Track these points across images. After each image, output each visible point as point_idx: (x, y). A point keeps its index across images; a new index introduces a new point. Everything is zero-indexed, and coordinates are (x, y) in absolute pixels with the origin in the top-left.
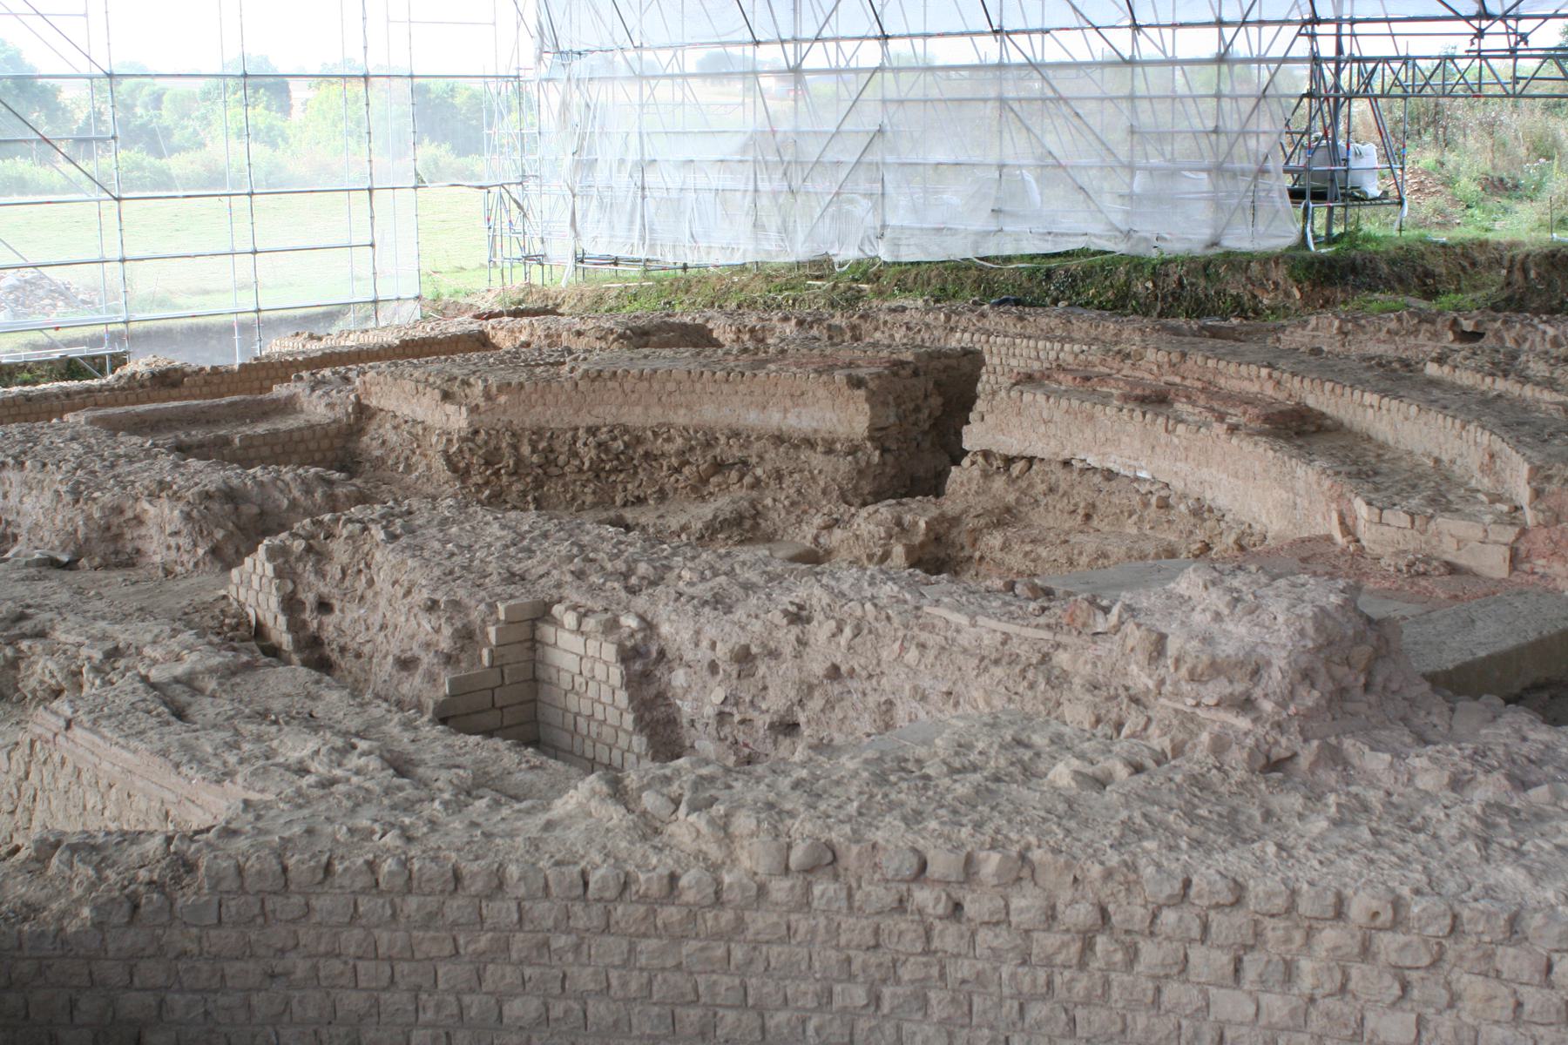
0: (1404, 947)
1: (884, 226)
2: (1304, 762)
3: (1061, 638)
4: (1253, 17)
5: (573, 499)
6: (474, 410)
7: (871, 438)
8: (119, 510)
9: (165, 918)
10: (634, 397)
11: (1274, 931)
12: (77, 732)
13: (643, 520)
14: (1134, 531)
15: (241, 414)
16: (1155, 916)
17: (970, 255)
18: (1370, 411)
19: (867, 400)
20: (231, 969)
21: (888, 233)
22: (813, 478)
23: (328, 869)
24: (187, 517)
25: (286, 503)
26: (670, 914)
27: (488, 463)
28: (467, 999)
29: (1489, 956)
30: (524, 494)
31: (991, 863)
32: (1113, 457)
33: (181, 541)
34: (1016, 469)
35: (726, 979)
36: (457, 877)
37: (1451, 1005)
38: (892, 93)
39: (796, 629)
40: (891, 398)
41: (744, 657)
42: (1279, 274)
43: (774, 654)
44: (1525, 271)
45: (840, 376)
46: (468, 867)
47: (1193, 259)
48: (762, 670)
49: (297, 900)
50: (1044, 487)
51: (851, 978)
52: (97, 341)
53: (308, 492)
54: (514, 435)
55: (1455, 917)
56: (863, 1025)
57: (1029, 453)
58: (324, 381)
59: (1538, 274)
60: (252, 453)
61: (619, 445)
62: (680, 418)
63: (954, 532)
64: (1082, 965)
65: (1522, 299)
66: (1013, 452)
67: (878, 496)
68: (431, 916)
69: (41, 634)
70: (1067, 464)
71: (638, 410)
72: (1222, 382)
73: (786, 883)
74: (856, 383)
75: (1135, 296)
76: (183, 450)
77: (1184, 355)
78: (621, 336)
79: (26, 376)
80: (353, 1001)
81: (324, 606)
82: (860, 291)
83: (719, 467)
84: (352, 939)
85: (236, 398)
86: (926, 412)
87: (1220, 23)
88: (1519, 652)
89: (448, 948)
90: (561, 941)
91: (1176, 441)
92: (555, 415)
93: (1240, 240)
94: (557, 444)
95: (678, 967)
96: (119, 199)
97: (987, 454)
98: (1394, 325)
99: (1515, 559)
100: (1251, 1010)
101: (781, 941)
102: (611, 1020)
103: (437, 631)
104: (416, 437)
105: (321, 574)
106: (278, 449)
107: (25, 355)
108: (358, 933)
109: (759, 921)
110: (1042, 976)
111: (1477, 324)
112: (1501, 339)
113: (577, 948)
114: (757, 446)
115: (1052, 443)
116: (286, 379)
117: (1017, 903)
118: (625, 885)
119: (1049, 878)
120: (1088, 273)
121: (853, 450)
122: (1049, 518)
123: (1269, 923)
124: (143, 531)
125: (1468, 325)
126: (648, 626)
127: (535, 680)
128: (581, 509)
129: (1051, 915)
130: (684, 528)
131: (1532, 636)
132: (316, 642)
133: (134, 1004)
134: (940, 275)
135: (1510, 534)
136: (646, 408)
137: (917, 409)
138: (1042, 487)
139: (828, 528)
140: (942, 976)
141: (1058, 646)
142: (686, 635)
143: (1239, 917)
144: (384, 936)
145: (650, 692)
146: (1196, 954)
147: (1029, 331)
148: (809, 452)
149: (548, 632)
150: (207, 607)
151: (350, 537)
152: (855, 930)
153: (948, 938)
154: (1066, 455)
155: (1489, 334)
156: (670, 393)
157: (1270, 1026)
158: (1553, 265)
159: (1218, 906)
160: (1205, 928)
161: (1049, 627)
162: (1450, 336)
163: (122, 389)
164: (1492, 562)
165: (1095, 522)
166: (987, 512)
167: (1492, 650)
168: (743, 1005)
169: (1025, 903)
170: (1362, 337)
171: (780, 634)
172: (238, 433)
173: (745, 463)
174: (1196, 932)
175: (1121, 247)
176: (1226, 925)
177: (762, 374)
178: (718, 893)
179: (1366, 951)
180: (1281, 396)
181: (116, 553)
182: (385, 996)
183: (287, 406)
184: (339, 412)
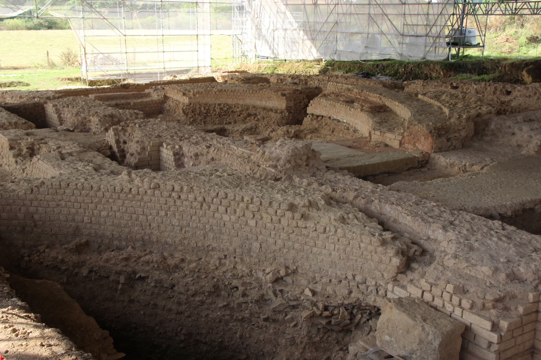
0: (253, 207)
1: (336, 50)
2: (283, 179)
3: (252, 153)
5: (213, 122)
6: (190, 98)
7: (286, 109)
8: (85, 118)
9: (38, 193)
10: (230, 96)
11: (233, 203)
12: (40, 161)
13: (229, 128)
14: (341, 135)
15: (135, 97)
16: (213, 200)
17: (359, 59)
19: (286, 99)
20: (50, 203)
22: (271, 119)
23: (68, 185)
24: (100, 121)
25: (125, 119)
26: (130, 196)
27: (193, 112)
28: (94, 211)
29: (267, 209)
30: (201, 120)
31: (185, 188)
33: (98, 126)
34: (320, 118)
35: (140, 209)
36: (92, 187)
37: (261, 219)
38: (340, 11)
39: (207, 150)
40: (292, 99)
41: (196, 155)
42: (438, 67)
43: (202, 155)
44: (505, 68)
45: (279, 93)
46: (94, 185)
47: (416, 63)
48: (200, 158)
49: (62, 190)
51: (162, 210)
52: (120, 75)
53: (131, 116)
55: (261, 202)
56: (164, 219)
57: (322, 114)
58: (158, 89)
60: (136, 107)
61: (225, 109)
62: (241, 102)
63: (301, 134)
64: (201, 209)
65: (503, 76)
66: (318, 114)
67: (287, 124)
68: (87, 195)
69: (46, 143)
70: (330, 118)
71: (231, 100)
72: (369, 98)
73: (150, 191)
74: (283, 95)
75: (399, 73)
76: (117, 106)
77: (362, 90)
78: (242, 80)
79: (99, 83)
80: (73, 211)
81: (125, 142)
82: (328, 69)
83: (249, 115)
84: (73, 199)
85: (135, 92)
86: (303, 103)
88: (379, 164)
89: (90, 201)
90: (111, 200)
92: (210, 100)
93: (431, 57)
94: (210, 108)
95: (132, 206)
96: (125, 36)
97: (312, 115)
98: (436, 84)
99: (401, 144)
100: (229, 219)
101: (149, 202)
102: (120, 216)
103: (138, 147)
104: (177, 104)
105: (124, 135)
106: (143, 106)
107: (101, 78)
108: (74, 197)
109: (146, 198)
110: (194, 211)
112: (463, 89)
113: (114, 202)
114: (259, 110)
116: (148, 88)
117: (190, 196)
118: (122, 190)
119: (196, 192)
120: (388, 66)
121: (282, 112)
122: (325, 131)
123: (231, 202)
124: (91, 124)
125: (455, 85)
126: (181, 147)
127: (159, 159)
128: (215, 124)
129: (196, 199)
130: (237, 130)
131: (385, 160)
132: (123, 151)
133: (32, 209)
134: (349, 65)
135: (400, 138)
137: (300, 102)
138: (324, 124)
139: (272, 132)
140: (178, 210)
141: (251, 154)
142: (187, 150)
143: (227, 201)
144: (79, 198)
145: (180, 163)
146: (220, 207)
147: (348, 82)
149: (161, 148)
150: (100, 142)
151: (131, 126)
152: (162, 200)
153: (178, 203)
154: (329, 115)
155: (460, 87)
157: (232, 222)
158: (512, 67)
159: (223, 198)
160: (221, 202)
161: (250, 150)
162: (450, 87)
163: (113, 89)
164: (395, 144)
165: (334, 133)
166: (310, 129)
167: (371, 163)
168: (143, 214)
169: (191, 196)
170: (428, 87)
171: (204, 150)
172: (132, 102)
173: (256, 114)
174: (219, 203)
176: (225, 202)
177: (261, 92)
178: (138, 192)
179: (247, 208)
180: (380, 102)
181: (85, 129)
182: (79, 210)
183: (148, 95)
184: (160, 97)
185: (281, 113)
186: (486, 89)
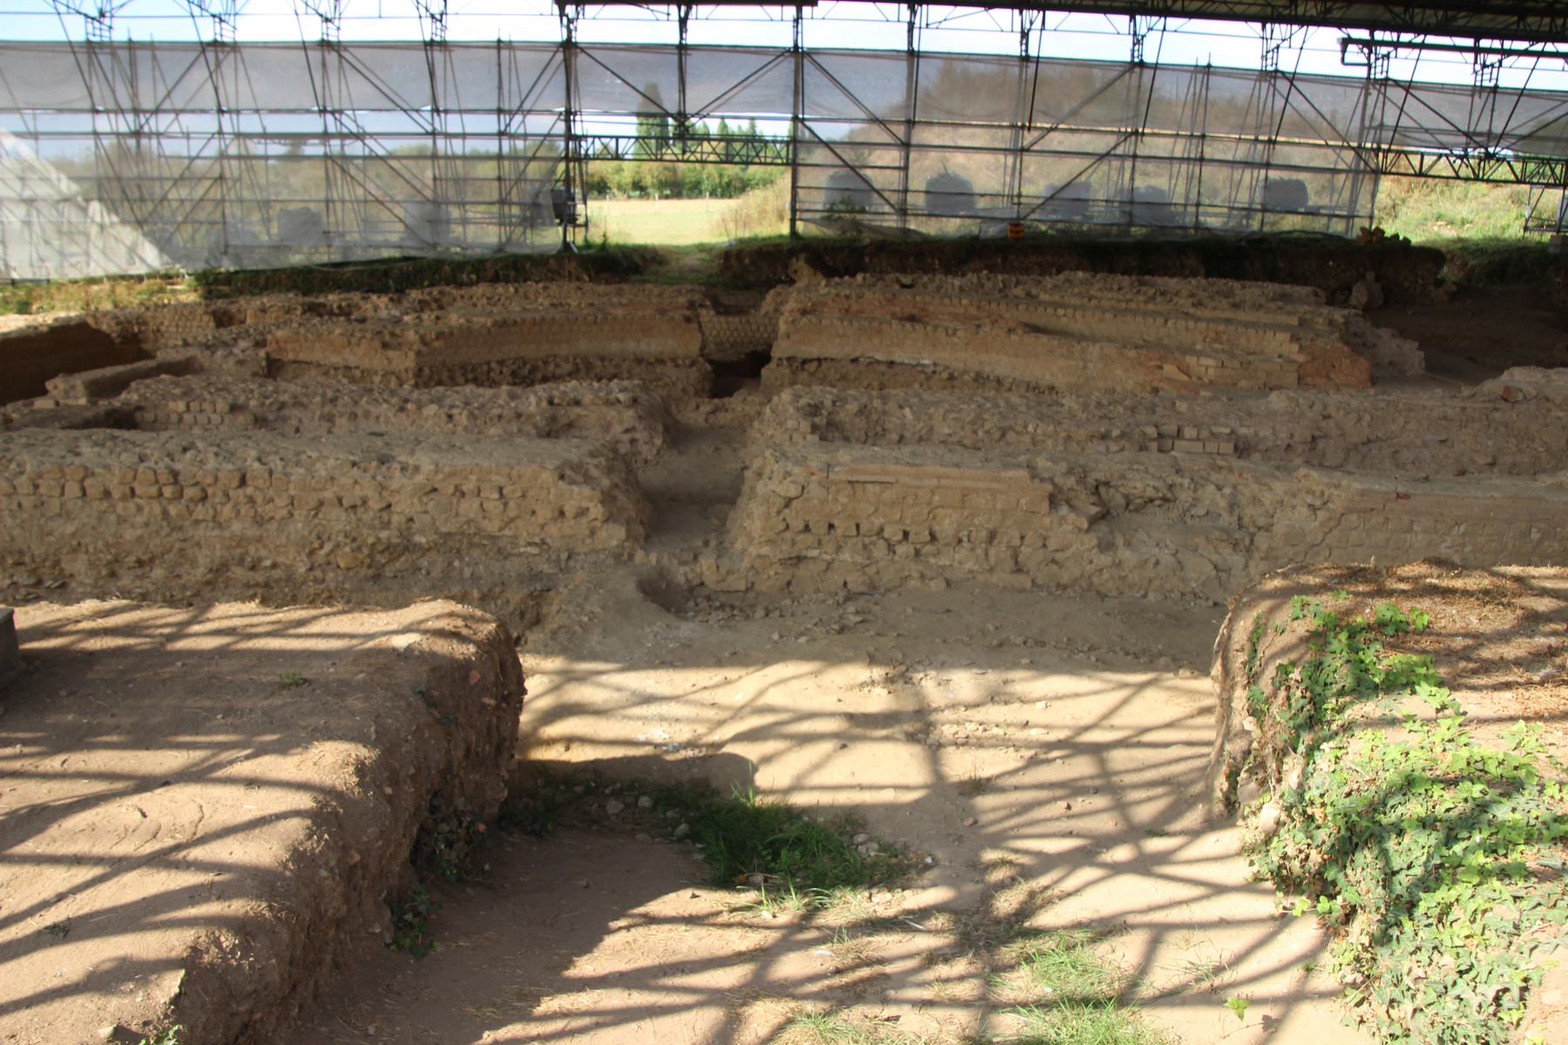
4: (527, 106)
18: (1065, 320)
21: (231, 251)
43: (1326, 436)
57: (823, 356)
62: (563, 350)
70: (855, 360)
87: (500, 111)
97: (790, 359)
114: (625, 366)
115: (847, 348)
139: (714, 412)
154: (857, 354)
175: (430, 255)
185: (693, 364)
186: (982, 286)
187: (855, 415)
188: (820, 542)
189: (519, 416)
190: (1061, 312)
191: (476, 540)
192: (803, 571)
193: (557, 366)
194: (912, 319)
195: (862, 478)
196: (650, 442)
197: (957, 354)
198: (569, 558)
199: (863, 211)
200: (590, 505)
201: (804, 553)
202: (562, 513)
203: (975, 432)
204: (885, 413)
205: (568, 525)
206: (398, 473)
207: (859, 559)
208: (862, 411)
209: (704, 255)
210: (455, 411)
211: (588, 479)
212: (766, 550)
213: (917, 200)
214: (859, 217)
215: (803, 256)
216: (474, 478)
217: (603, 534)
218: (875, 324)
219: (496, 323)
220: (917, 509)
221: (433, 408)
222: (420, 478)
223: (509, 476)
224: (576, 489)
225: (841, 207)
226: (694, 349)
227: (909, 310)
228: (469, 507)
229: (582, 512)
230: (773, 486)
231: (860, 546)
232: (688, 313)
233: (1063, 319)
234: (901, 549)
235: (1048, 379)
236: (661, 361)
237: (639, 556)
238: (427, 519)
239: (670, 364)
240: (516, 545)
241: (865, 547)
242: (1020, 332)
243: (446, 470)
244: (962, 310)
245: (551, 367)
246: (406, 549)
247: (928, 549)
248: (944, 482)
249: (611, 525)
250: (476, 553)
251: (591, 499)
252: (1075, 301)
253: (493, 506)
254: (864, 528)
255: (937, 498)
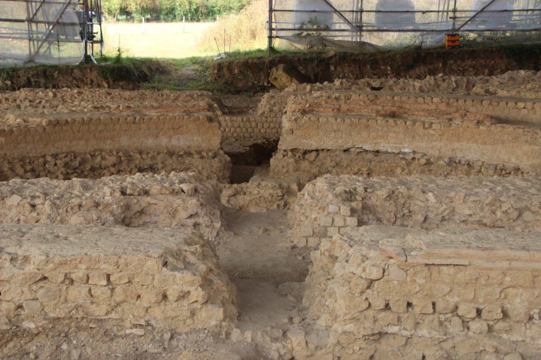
32: (382, 145)
50: (333, 163)
54: (9, 163)
59: (240, 71)
62: (108, 145)
71: (82, 142)
91: (432, 132)
111: (381, 83)
114: (160, 158)
115: (340, 141)
136: (87, 140)
148: (190, 159)
154: (349, 145)
156: (100, 132)
186: (438, 86)
187: (385, 199)
188: (399, 319)
189: (97, 205)
190: (521, 105)
191: (84, 323)
192: (385, 345)
193: (103, 158)
194: (393, 115)
195: (437, 261)
196: (210, 226)
197: (432, 143)
198: (172, 337)
199: (327, 29)
200: (192, 289)
201: (385, 329)
202: (165, 297)
203: (494, 213)
204: (409, 197)
205: (170, 308)
206: (7, 264)
207: (437, 335)
208: (391, 196)
209: (197, 67)
210: (37, 201)
211: (187, 266)
212: (350, 327)
213: (368, 18)
214: (324, 33)
215: (281, 66)
216: (83, 267)
217: (202, 314)
218: (364, 121)
219: (50, 123)
220: (489, 289)
221: (15, 199)
222: (30, 268)
223: (117, 265)
224: (178, 274)
225: (309, 26)
226: (216, 142)
227: (389, 108)
228: (78, 294)
229: (184, 295)
230: (351, 268)
231: (436, 322)
232: (210, 114)
233: (523, 111)
234: (475, 326)
235: (513, 162)
236: (189, 154)
237: (236, 334)
238: (36, 305)
239: (196, 156)
240: (123, 328)
241: (441, 323)
242: (488, 123)
243: (57, 260)
244: (433, 107)
245: (99, 159)
246: (15, 335)
247: (500, 325)
248: (514, 264)
249: (210, 307)
250: (83, 336)
251: (192, 283)
252: (528, 95)
253: (101, 290)
254: (440, 306)
255: (508, 279)
